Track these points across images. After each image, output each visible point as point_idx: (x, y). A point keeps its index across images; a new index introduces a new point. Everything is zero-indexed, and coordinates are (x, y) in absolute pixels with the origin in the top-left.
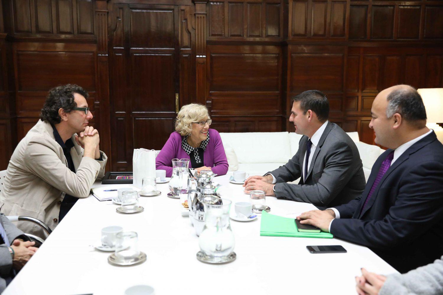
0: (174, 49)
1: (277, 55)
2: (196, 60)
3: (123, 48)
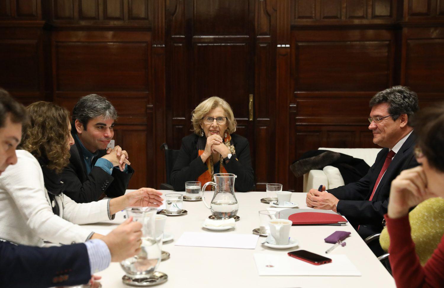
0: (248, 36)
1: (387, 42)
3: (184, 36)
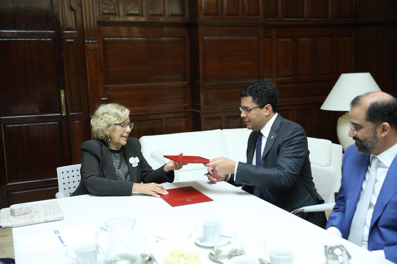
0: (54, 32)
2: (86, 46)
